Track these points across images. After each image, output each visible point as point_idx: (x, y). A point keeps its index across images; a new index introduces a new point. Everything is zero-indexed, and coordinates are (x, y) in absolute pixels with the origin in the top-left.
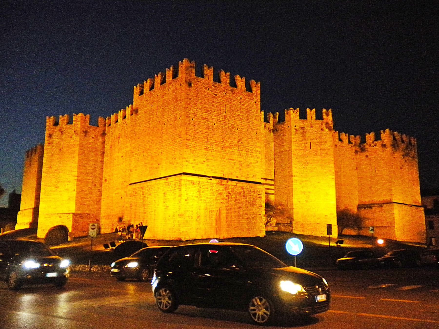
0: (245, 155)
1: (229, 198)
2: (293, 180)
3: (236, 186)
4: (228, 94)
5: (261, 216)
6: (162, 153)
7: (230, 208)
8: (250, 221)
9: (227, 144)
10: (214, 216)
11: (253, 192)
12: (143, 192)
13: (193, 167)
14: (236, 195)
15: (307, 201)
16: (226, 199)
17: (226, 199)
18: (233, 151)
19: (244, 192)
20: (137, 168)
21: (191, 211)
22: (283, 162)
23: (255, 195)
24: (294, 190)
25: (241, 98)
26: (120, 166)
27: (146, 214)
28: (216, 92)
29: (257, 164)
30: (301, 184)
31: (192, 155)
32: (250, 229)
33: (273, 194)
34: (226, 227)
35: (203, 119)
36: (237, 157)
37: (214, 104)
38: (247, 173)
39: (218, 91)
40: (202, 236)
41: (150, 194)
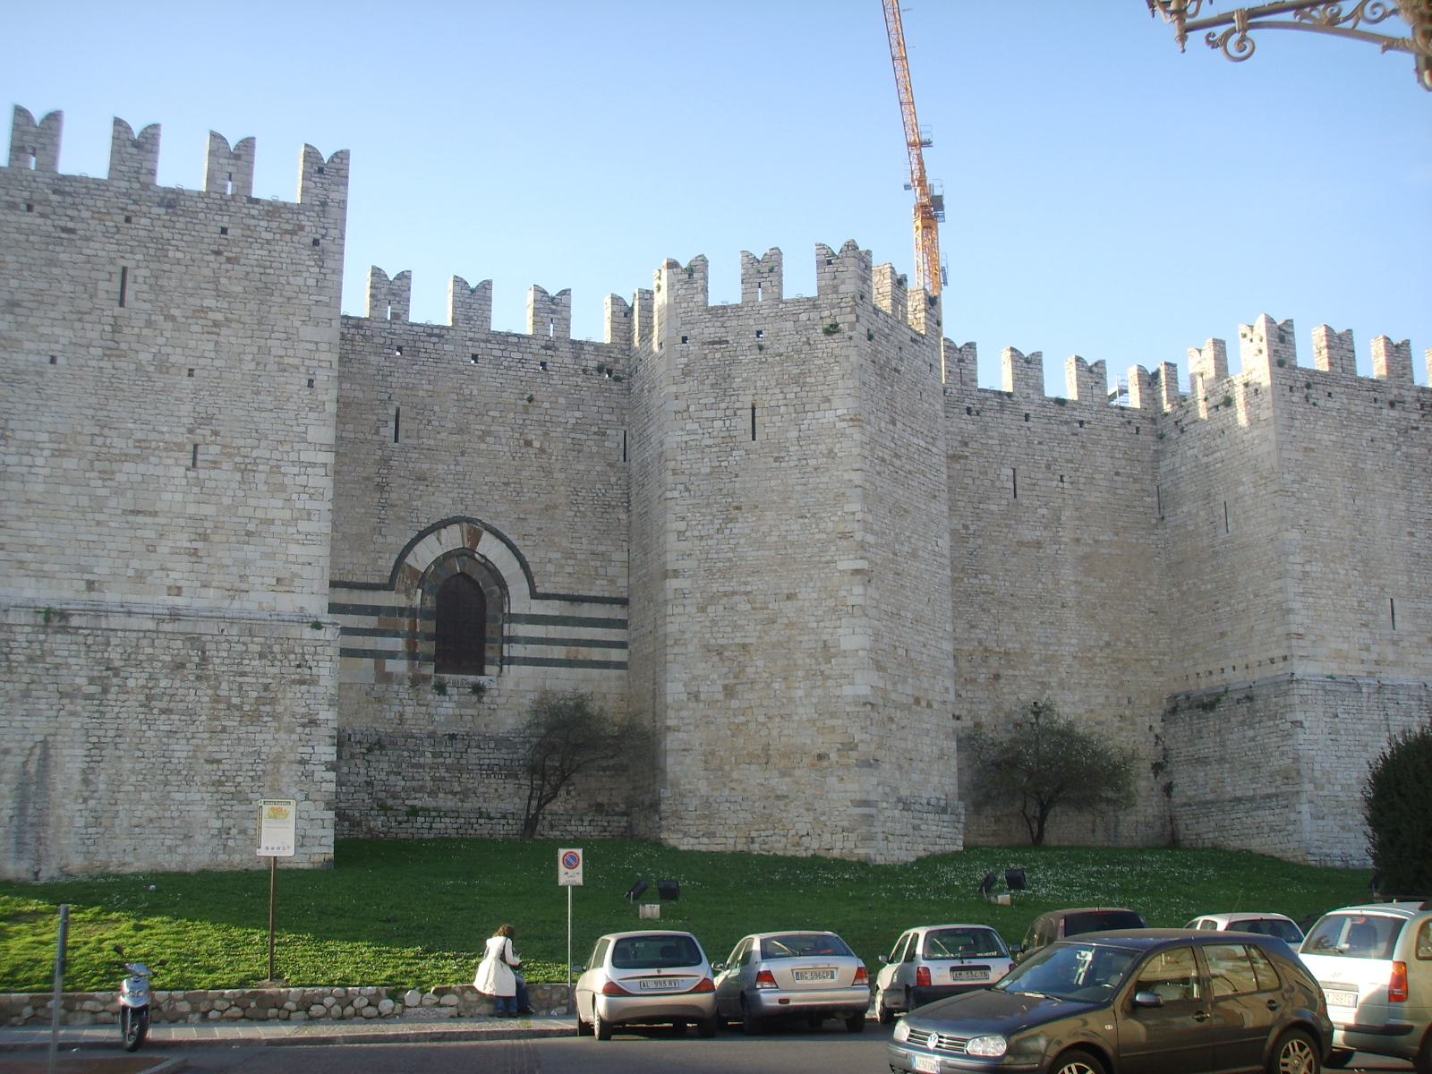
0: (235, 485)
1: (105, 691)
2: (670, 595)
3: (157, 632)
4: (144, 221)
7: (111, 733)
8: (233, 796)
9: (119, 443)
11: (262, 656)
14: (150, 678)
15: (729, 692)
18: (160, 471)
19: (204, 659)
23: (275, 670)
24: (670, 642)
28: (72, 218)
29: (304, 526)
30: (702, 609)
32: (234, 831)
33: (620, 665)
34: (80, 822)
36: (179, 497)
37: (56, 271)
38: (234, 570)
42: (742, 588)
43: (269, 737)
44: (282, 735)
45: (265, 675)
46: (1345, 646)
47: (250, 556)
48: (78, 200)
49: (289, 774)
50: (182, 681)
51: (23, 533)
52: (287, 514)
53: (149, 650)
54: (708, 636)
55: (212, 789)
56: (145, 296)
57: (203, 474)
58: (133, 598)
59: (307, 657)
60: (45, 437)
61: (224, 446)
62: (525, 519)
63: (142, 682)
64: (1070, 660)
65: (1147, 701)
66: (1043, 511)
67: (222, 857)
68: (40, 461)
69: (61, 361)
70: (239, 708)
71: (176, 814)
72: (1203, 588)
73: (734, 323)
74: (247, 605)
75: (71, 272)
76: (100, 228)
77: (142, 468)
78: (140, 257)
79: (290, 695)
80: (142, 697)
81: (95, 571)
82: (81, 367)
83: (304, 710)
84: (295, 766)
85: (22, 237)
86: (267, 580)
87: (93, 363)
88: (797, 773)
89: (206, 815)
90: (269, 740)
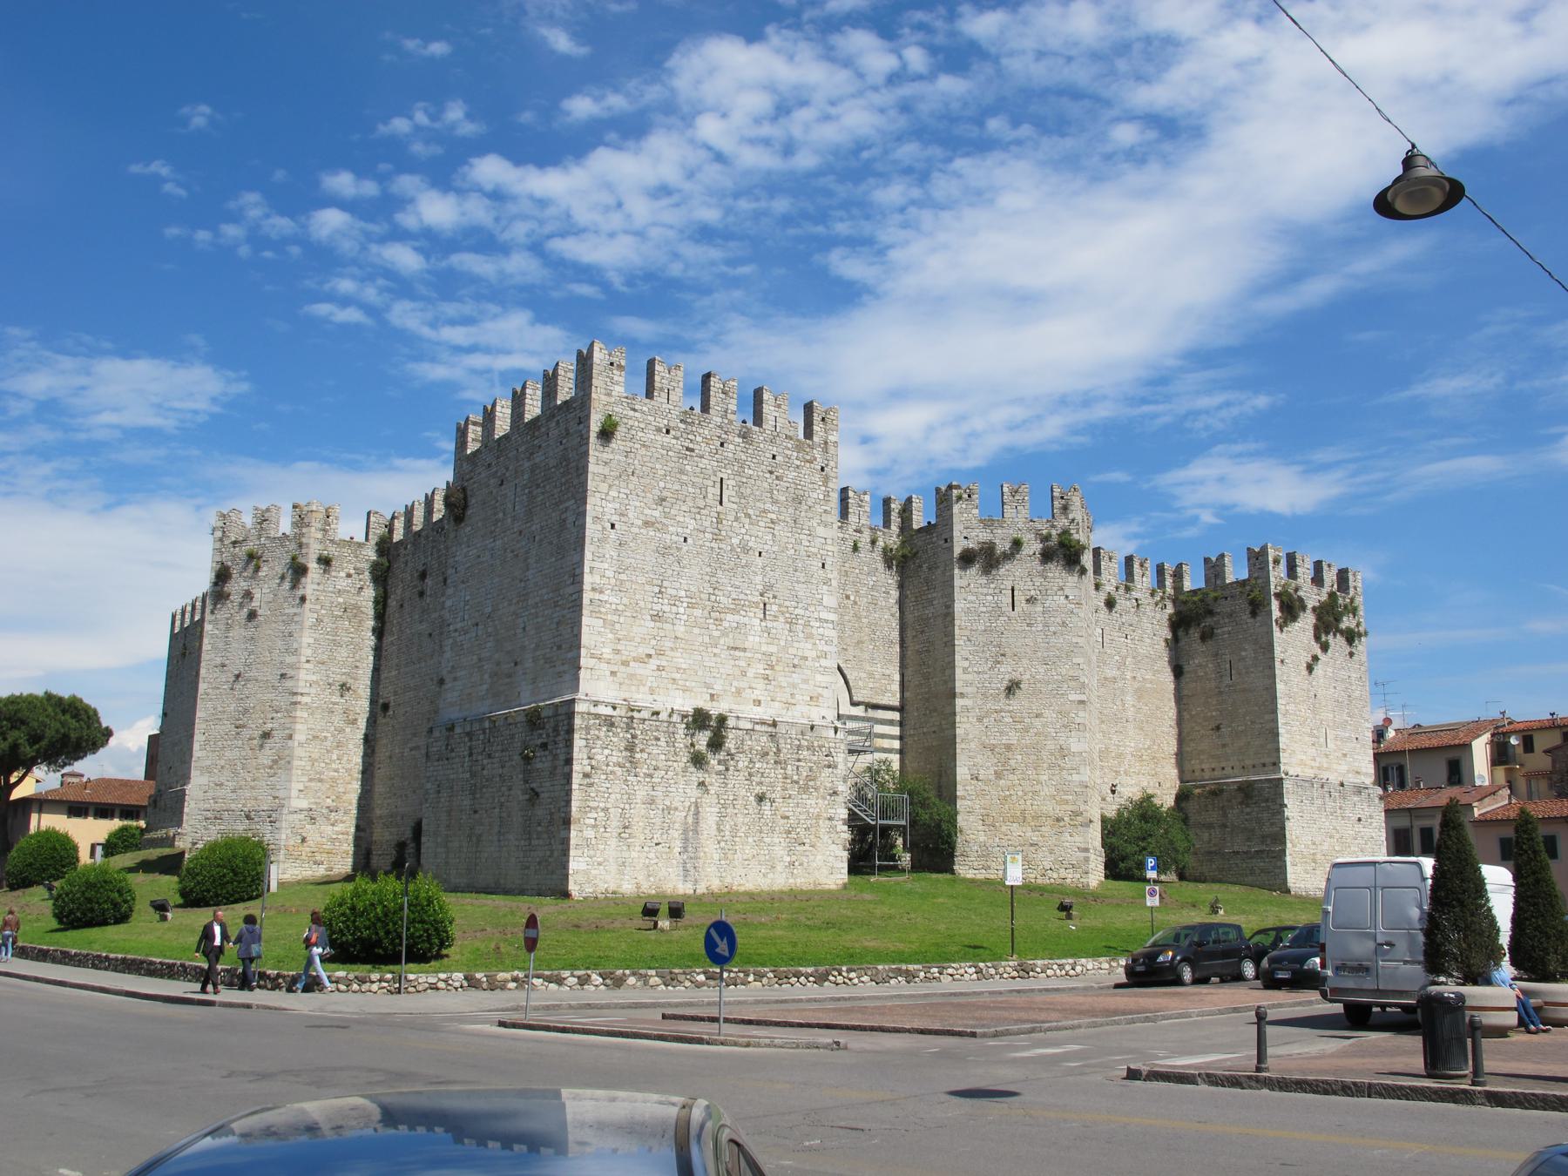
0: (787, 633)
1: (727, 769)
2: (958, 709)
3: (753, 730)
4: (731, 447)
5: (834, 822)
6: (524, 628)
7: (731, 797)
10: (677, 826)
12: (470, 748)
13: (613, 673)
14: (751, 761)
15: (998, 775)
16: (719, 773)
17: (719, 773)
18: (746, 620)
20: (459, 674)
21: (603, 810)
22: (928, 651)
23: (815, 758)
25: (774, 457)
26: (423, 664)
27: (477, 816)
29: (824, 662)
31: (610, 636)
32: (796, 864)
34: (716, 856)
35: (647, 524)
36: (757, 639)
37: (685, 477)
39: (699, 439)
40: (638, 888)
41: (489, 756)
42: (1007, 708)
43: (813, 802)
44: (820, 801)
45: (810, 761)
46: (1304, 757)
47: (796, 681)
48: (694, 429)
49: (824, 824)
50: (767, 763)
51: (675, 660)
52: (814, 654)
53: (749, 743)
54: (984, 738)
55: (785, 836)
56: (733, 499)
57: (770, 624)
58: (734, 707)
59: (832, 750)
60: (683, 593)
61: (780, 606)
62: (846, 650)
63: (746, 764)
64: (1129, 757)
65: (1168, 785)
66: (1117, 658)
67: (791, 881)
68: (681, 610)
69: (689, 540)
70: (797, 782)
71: (766, 852)
72: (1209, 714)
73: (999, 531)
74: (796, 714)
75: (692, 478)
76: (707, 449)
77: (737, 618)
78: (729, 471)
79: (823, 775)
80: (746, 774)
81: (715, 687)
82: (701, 546)
83: (829, 785)
84: (827, 822)
85: (665, 452)
86: (805, 698)
87: (707, 544)
88: (1043, 829)
89: (782, 852)
90: (814, 803)
